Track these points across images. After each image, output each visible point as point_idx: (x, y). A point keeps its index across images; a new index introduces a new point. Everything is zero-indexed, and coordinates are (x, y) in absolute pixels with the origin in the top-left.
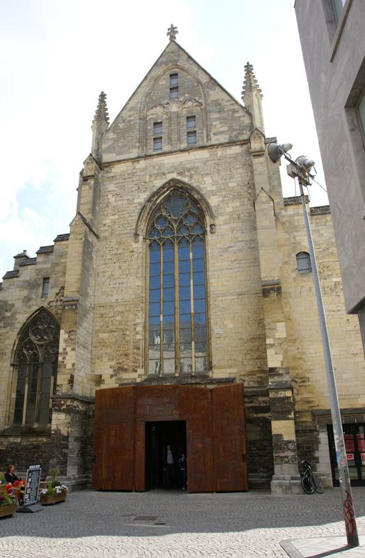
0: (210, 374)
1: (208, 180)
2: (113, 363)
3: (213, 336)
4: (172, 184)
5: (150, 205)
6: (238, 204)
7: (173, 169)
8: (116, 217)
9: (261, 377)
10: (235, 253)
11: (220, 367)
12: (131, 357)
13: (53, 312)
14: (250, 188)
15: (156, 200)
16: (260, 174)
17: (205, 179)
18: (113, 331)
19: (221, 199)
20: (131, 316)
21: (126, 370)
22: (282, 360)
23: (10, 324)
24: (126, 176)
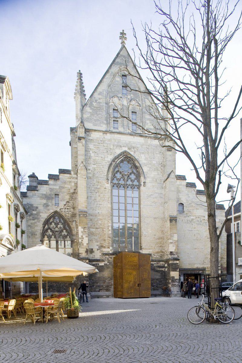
0: (141, 251)
1: (143, 156)
2: (98, 244)
3: (143, 235)
4: (125, 154)
5: (114, 164)
6: (156, 173)
7: (125, 145)
8: (95, 166)
9: (161, 254)
10: (154, 198)
11: (146, 249)
12: (107, 241)
13: (63, 214)
14: (162, 166)
15: (117, 162)
16: (170, 161)
17: (142, 155)
18: (97, 228)
19: (148, 169)
20: (106, 222)
21: (104, 247)
22: (175, 249)
23: (36, 218)
24: (100, 142)
